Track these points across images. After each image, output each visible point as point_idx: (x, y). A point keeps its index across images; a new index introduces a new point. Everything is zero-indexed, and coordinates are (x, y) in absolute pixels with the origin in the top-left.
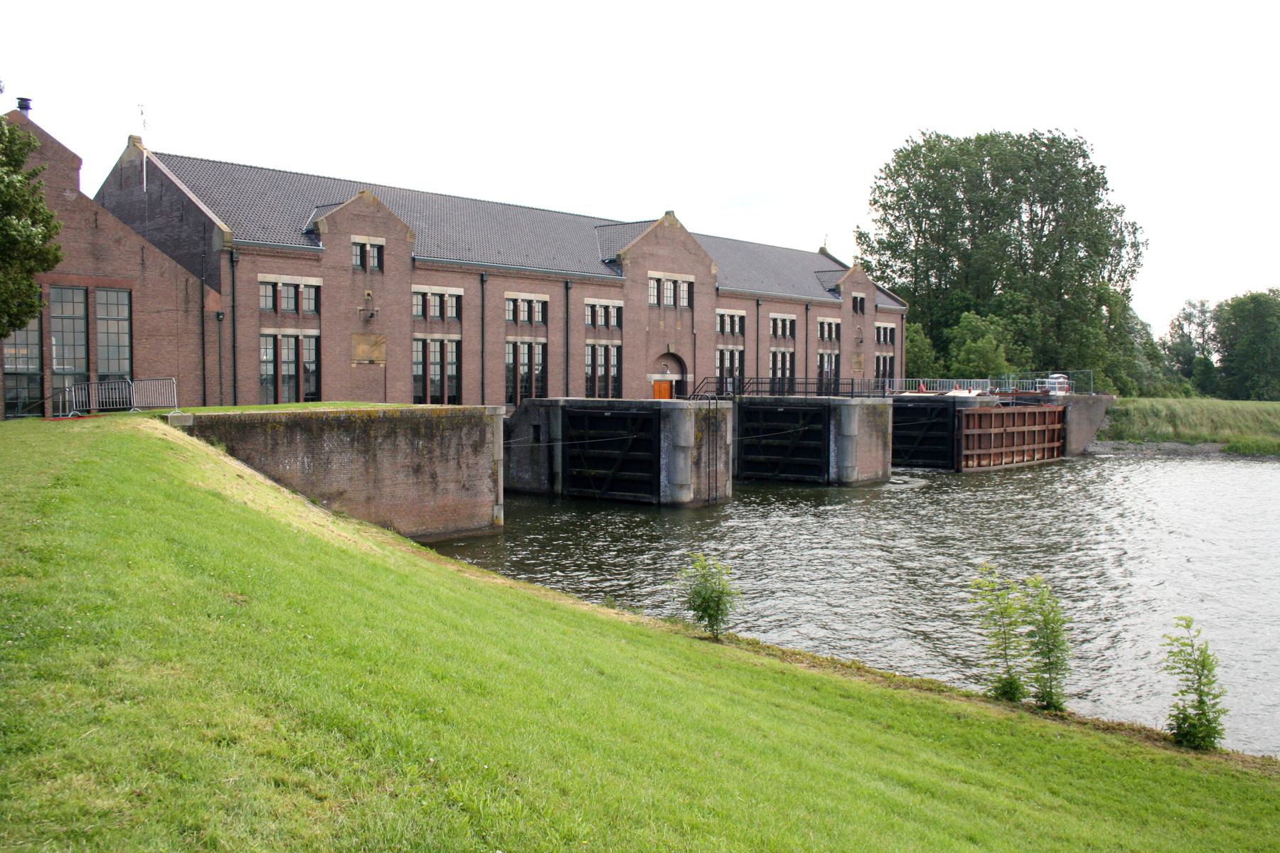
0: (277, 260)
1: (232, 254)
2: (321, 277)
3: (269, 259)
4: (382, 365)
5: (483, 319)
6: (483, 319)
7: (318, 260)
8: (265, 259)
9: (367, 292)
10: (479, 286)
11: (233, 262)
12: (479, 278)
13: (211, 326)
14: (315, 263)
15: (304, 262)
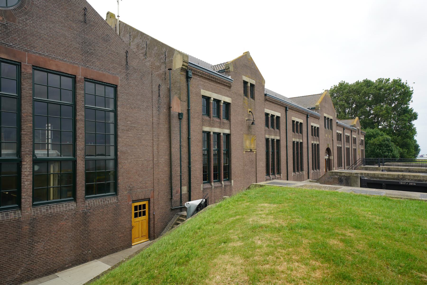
0: (211, 83)
1: (187, 72)
2: (230, 97)
3: (207, 81)
4: (255, 152)
5: (286, 129)
6: (286, 129)
7: (230, 87)
8: (205, 81)
9: (249, 110)
10: (285, 113)
11: (188, 78)
12: (285, 109)
13: (175, 121)
14: (228, 89)
15: (223, 87)
